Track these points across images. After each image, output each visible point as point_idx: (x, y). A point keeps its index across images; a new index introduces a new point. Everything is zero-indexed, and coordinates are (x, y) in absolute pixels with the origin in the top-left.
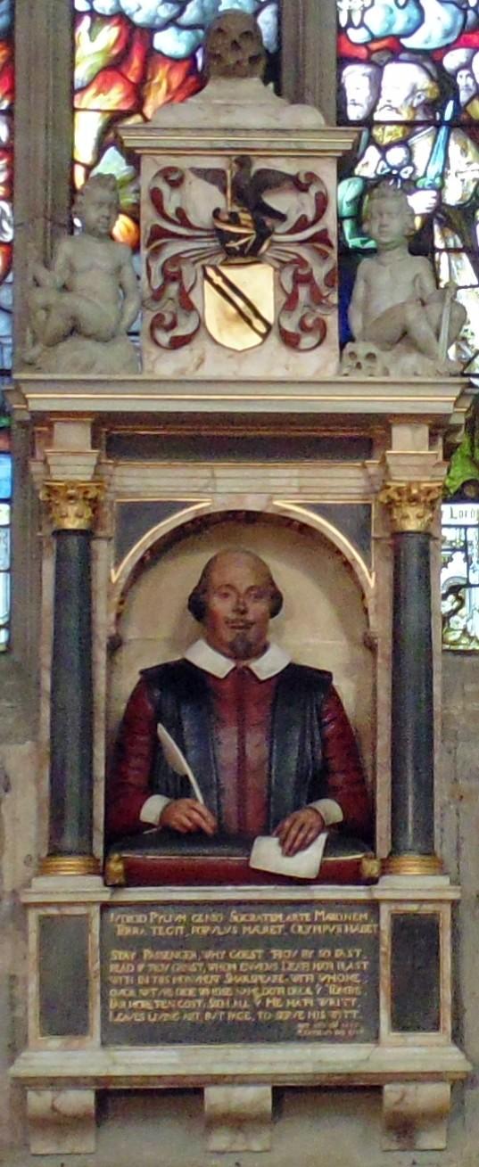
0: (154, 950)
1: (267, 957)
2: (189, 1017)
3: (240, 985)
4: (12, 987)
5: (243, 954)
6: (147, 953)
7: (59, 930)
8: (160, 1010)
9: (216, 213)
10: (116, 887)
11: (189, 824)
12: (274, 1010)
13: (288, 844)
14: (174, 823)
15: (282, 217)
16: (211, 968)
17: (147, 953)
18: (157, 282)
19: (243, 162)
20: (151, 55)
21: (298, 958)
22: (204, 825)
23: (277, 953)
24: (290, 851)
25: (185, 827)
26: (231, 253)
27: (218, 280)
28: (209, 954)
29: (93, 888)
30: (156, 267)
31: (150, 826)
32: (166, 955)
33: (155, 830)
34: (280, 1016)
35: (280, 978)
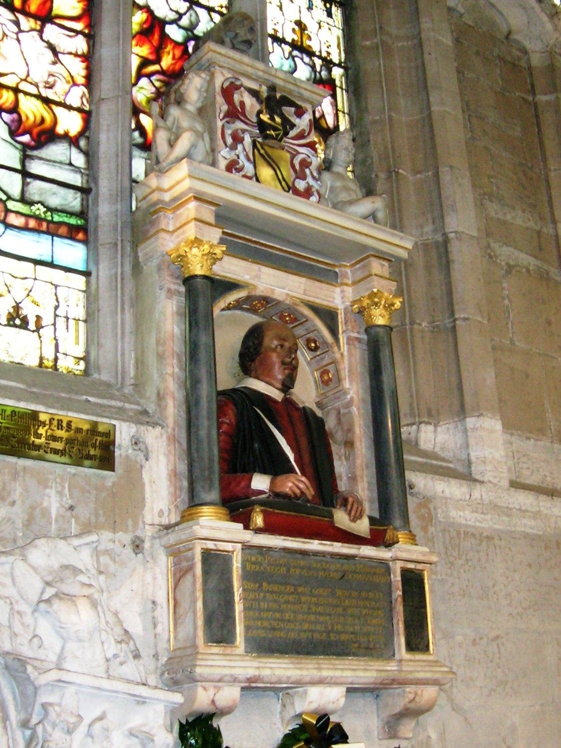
0: (269, 583)
1: (333, 594)
2: (293, 635)
3: (320, 614)
4: (153, 610)
5: (321, 591)
6: (265, 584)
7: (215, 562)
8: (274, 629)
9: (259, 112)
10: (258, 531)
11: (298, 492)
12: (339, 633)
13: (353, 513)
14: (288, 490)
15: (293, 126)
16: (303, 600)
17: (265, 584)
18: (229, 140)
19: (272, 88)
20: (165, 38)
21: (350, 597)
22: (307, 493)
23: (339, 592)
24: (354, 520)
25: (294, 493)
26: (266, 137)
27: (262, 151)
28: (300, 589)
29: (235, 530)
30: (228, 132)
31: (261, 492)
32: (275, 588)
33: (264, 496)
34: (343, 637)
35: (340, 610)
